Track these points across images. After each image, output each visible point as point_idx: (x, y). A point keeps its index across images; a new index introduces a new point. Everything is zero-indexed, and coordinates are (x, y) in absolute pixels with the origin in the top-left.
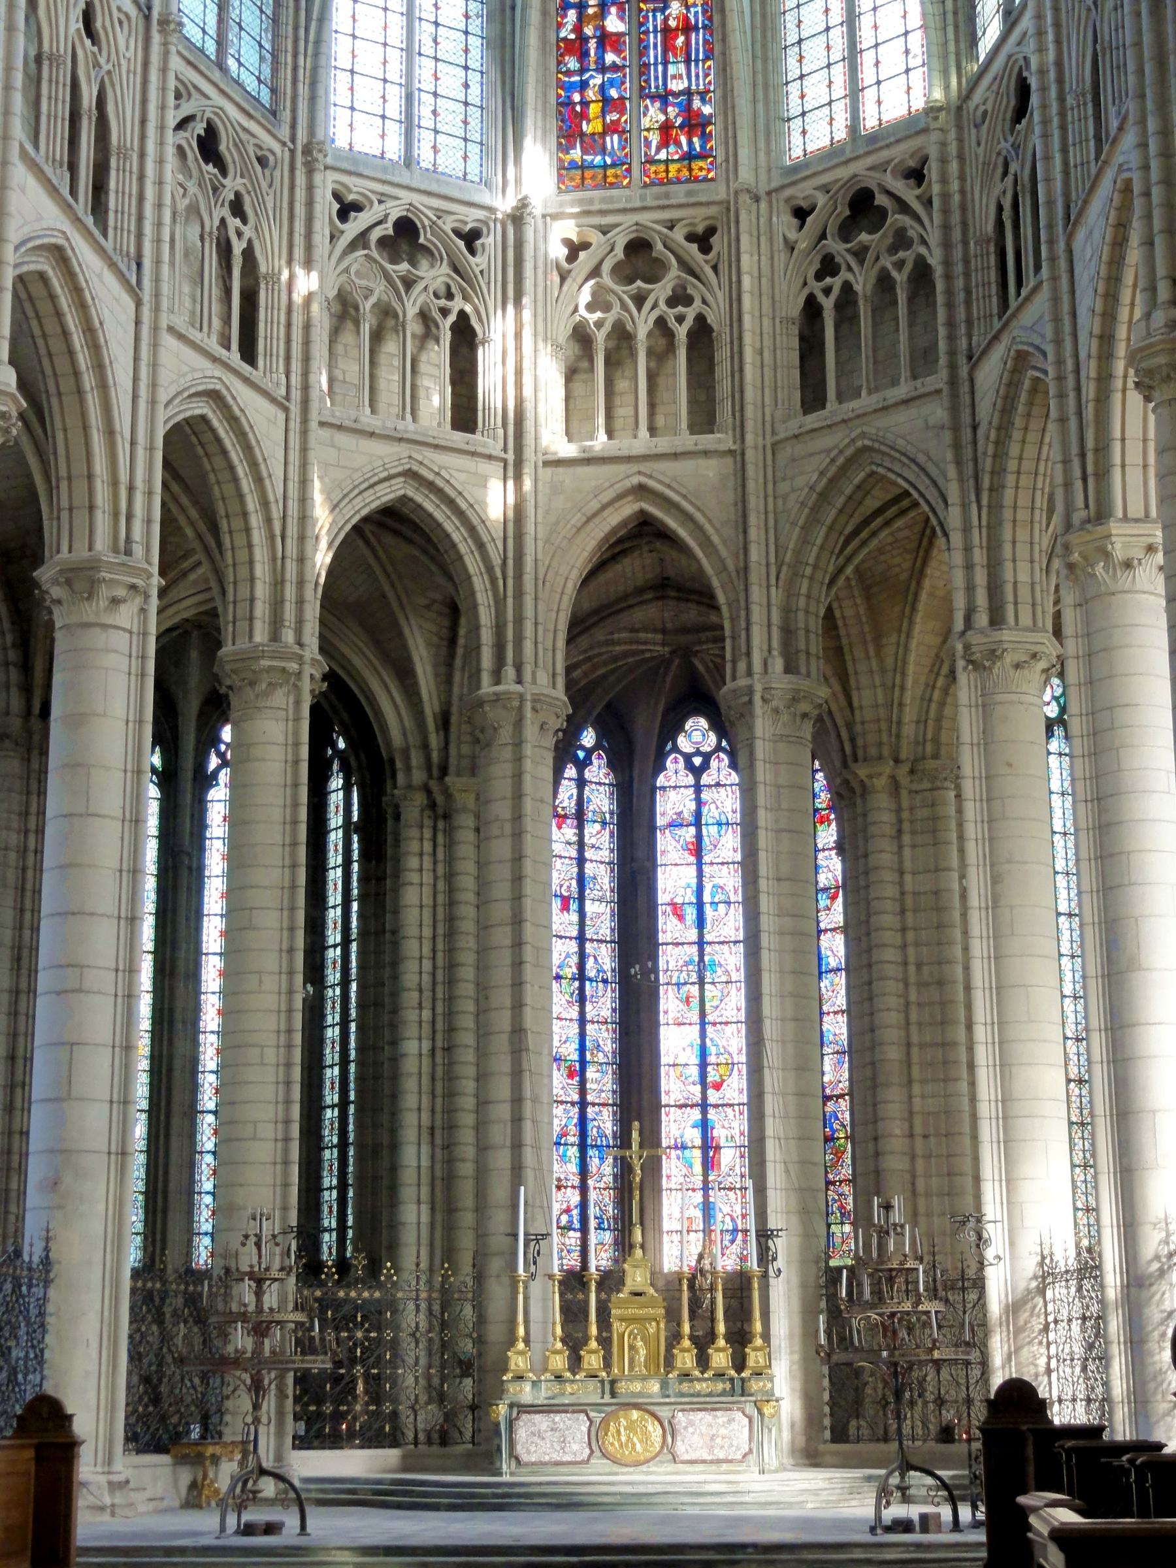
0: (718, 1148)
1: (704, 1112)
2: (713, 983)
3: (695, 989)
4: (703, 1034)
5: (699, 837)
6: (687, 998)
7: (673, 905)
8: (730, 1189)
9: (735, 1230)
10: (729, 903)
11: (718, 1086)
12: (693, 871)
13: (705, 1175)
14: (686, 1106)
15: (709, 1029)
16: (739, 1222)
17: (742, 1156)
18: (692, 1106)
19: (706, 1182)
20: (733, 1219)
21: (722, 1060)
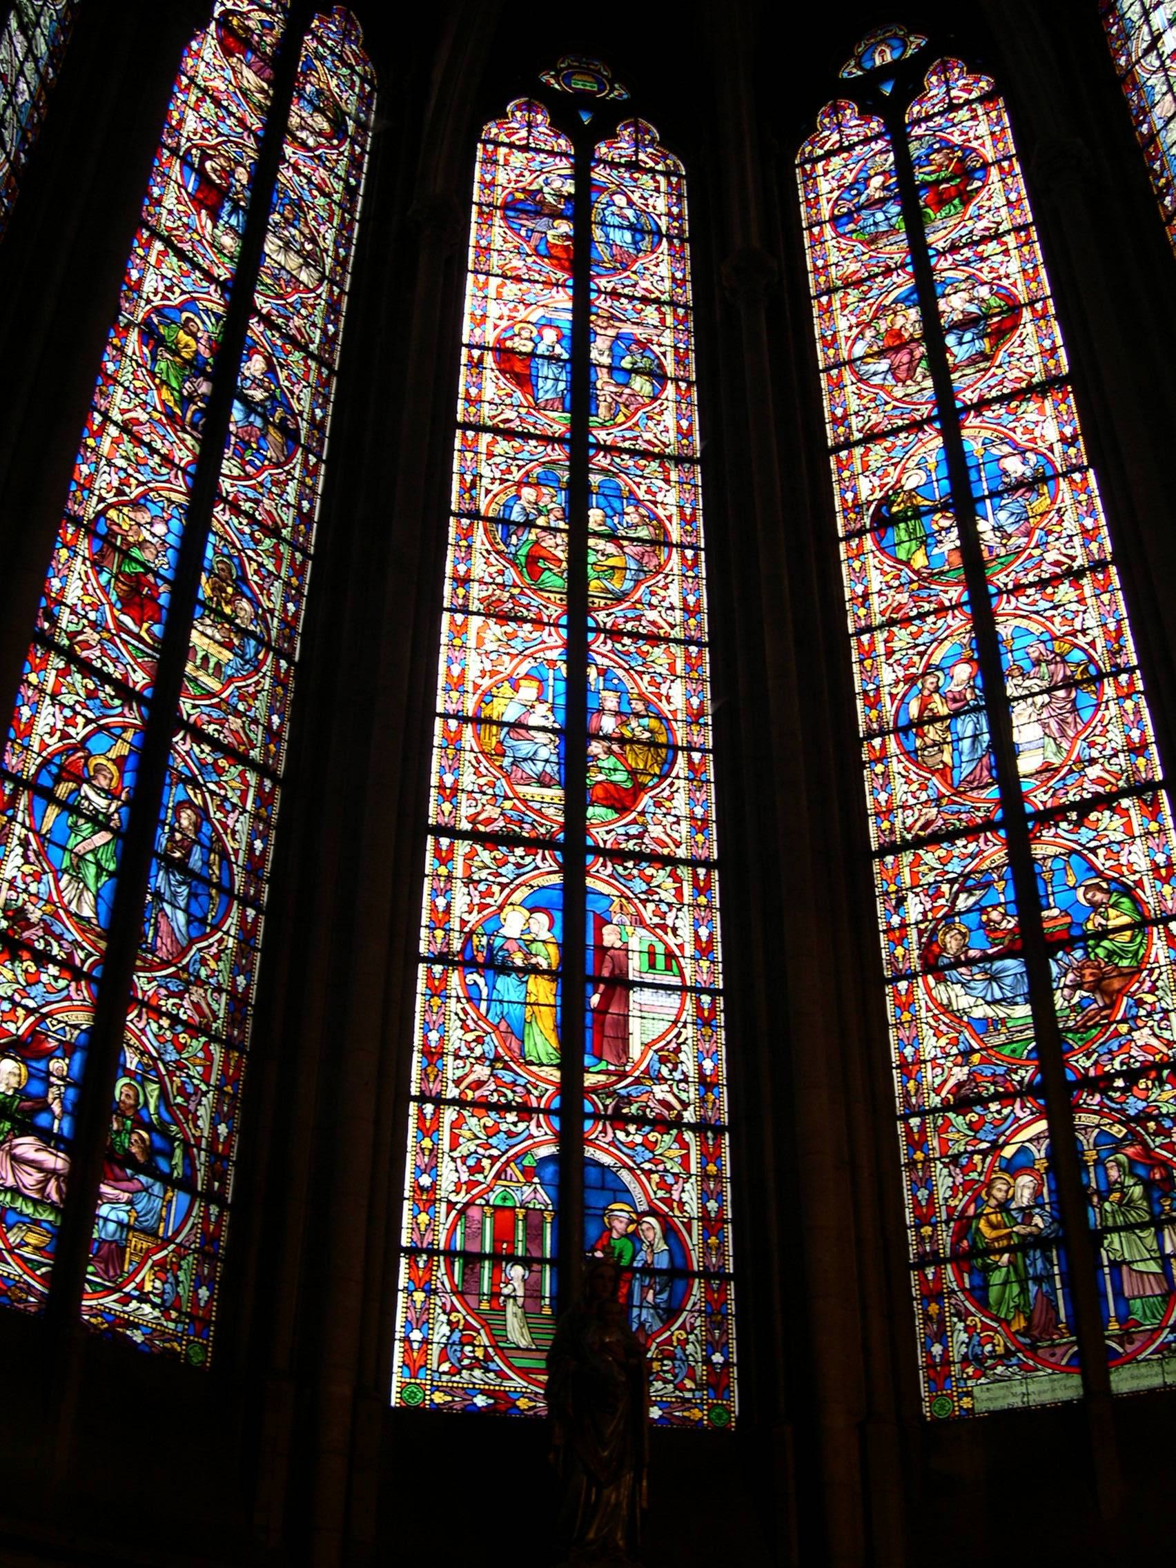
0: (620, 984)
1: (574, 873)
2: (612, 537)
3: (557, 546)
4: (577, 654)
5: (582, 239)
6: (532, 559)
7: (504, 354)
8: (662, 1125)
9: (679, 1273)
10: (658, 376)
11: (621, 801)
12: (563, 300)
13: (571, 1064)
14: (509, 840)
15: (600, 647)
16: (694, 1240)
17: (703, 1021)
18: (533, 845)
19: (571, 1087)
20: (669, 1230)
21: (636, 728)
